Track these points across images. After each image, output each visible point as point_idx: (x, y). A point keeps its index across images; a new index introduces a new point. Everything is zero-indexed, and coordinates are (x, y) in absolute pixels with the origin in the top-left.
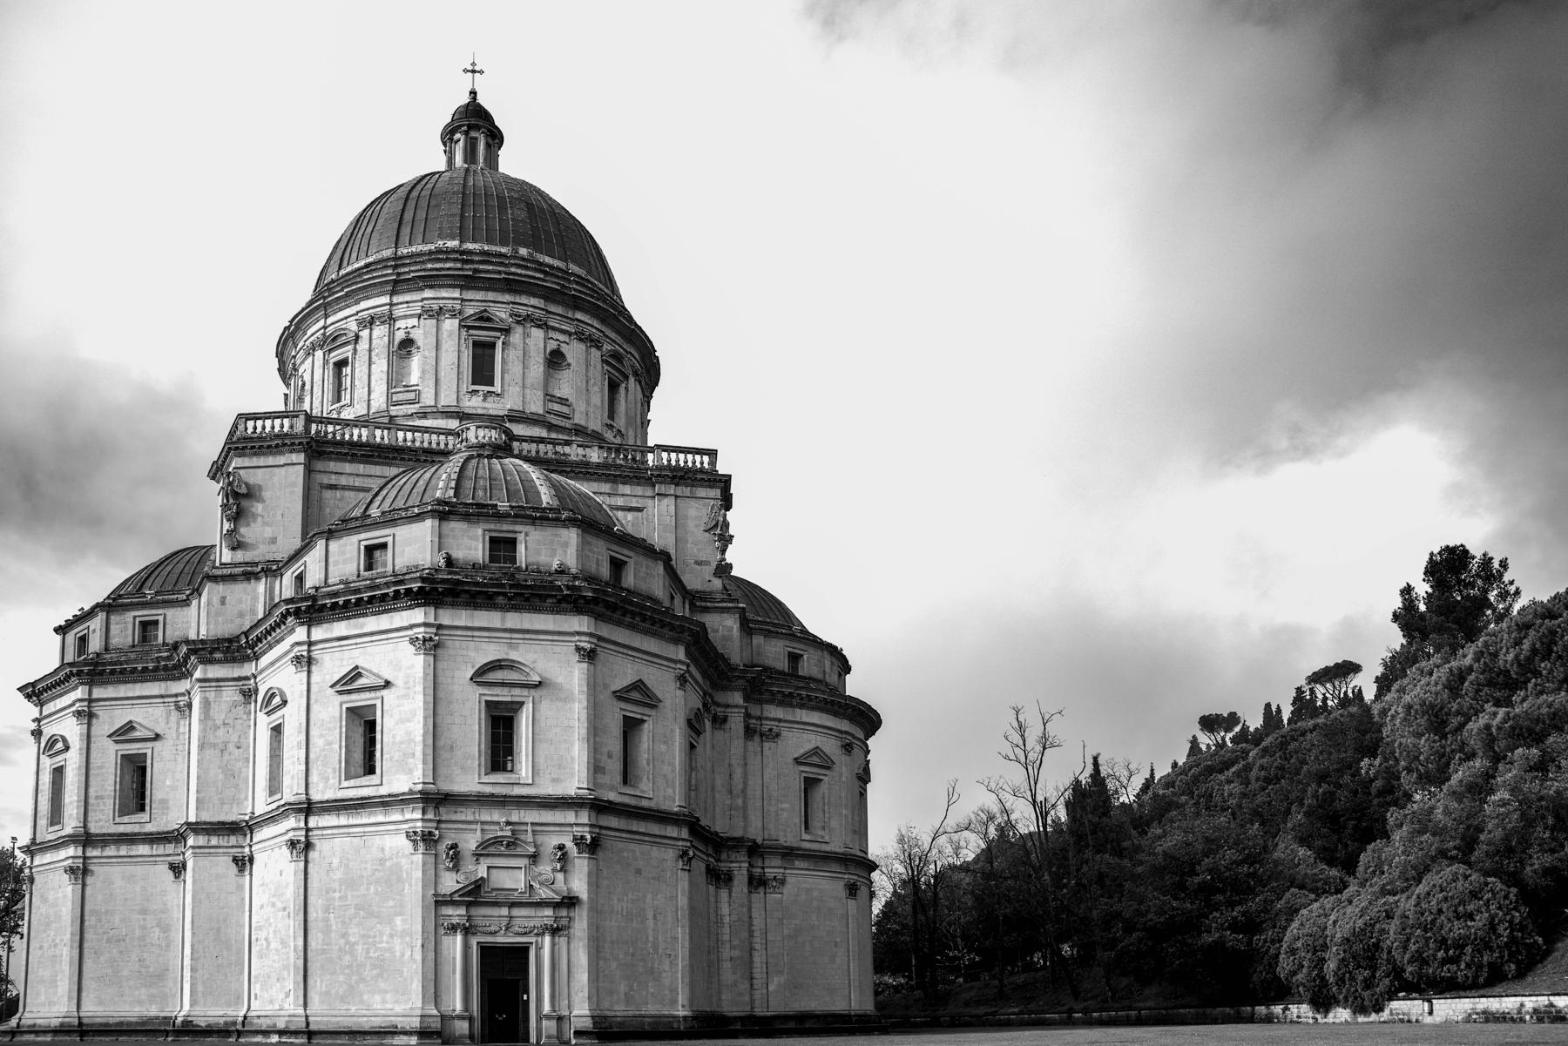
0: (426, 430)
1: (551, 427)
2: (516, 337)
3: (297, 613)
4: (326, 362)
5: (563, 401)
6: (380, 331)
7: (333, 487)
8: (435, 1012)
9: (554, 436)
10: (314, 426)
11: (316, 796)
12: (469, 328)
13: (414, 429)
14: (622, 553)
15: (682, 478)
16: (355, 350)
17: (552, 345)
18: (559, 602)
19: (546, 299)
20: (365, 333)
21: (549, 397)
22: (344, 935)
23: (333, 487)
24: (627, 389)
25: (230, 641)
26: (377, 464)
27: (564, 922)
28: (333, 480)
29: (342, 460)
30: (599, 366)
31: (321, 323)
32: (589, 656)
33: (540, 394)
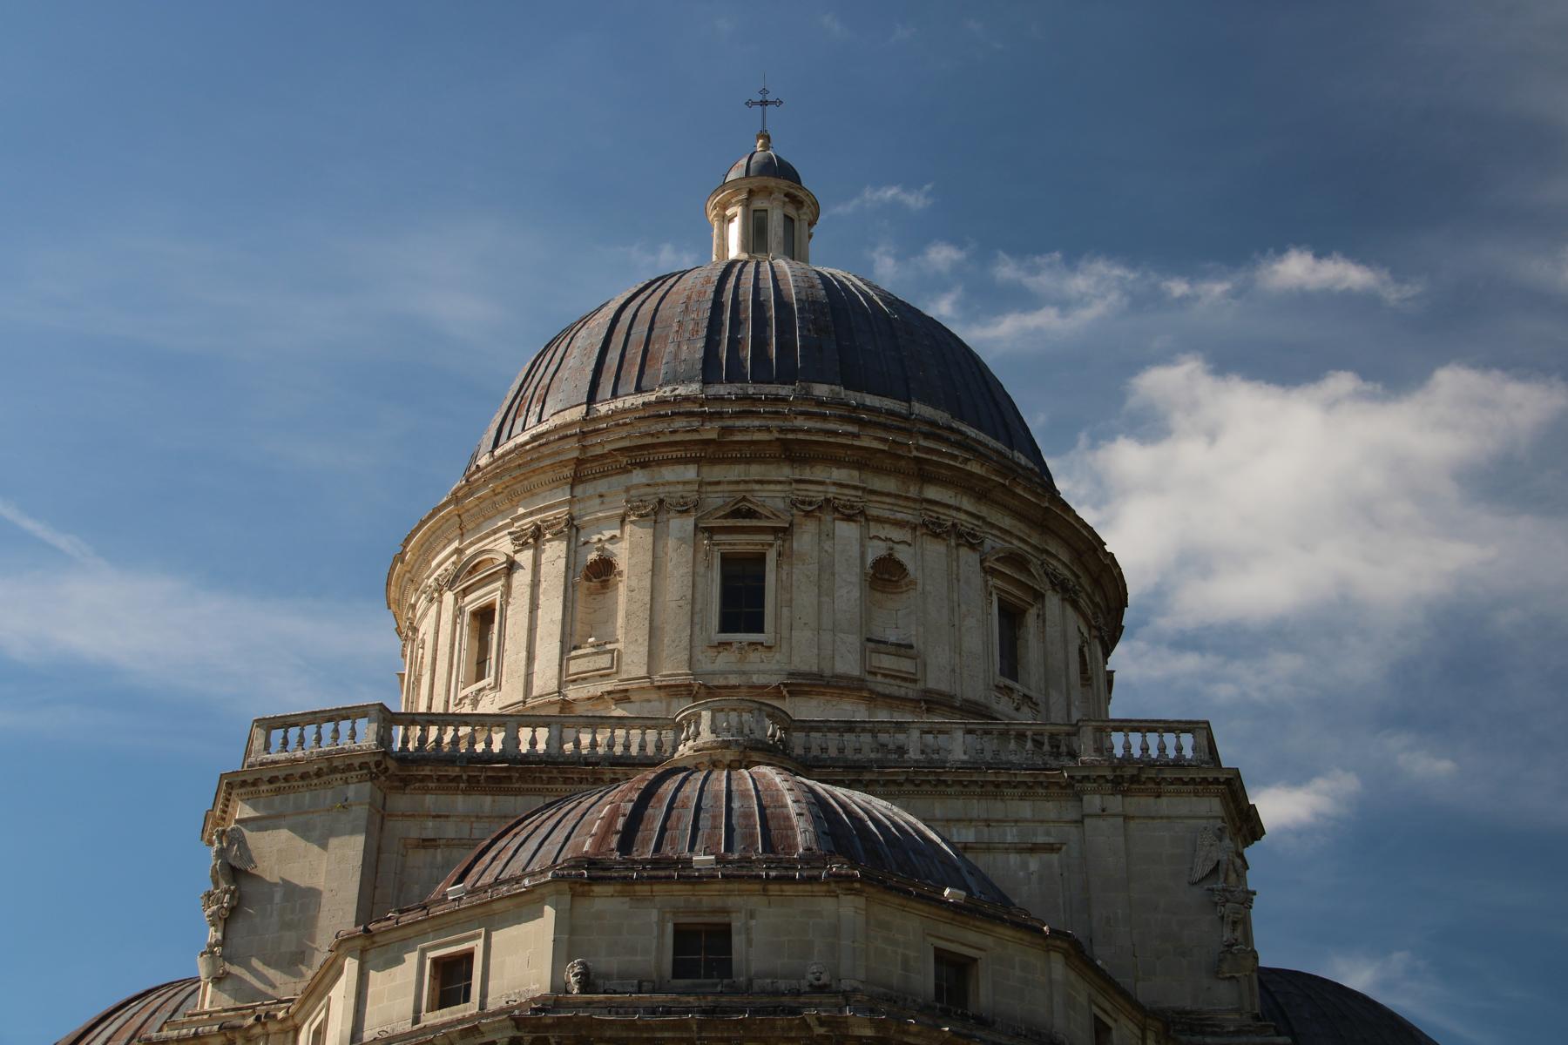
0: (620, 722)
1: (876, 698)
2: (805, 539)
4: (459, 612)
5: (903, 649)
7: (427, 843)
9: (883, 716)
10: (399, 731)
12: (711, 531)
13: (595, 723)
14: (967, 939)
15: (1134, 779)
17: (876, 550)
19: (860, 465)
20: (525, 558)
21: (874, 643)
23: (427, 843)
24: (1041, 617)
26: (518, 792)
28: (430, 829)
29: (446, 790)
30: (977, 579)
31: (456, 544)
33: (854, 640)
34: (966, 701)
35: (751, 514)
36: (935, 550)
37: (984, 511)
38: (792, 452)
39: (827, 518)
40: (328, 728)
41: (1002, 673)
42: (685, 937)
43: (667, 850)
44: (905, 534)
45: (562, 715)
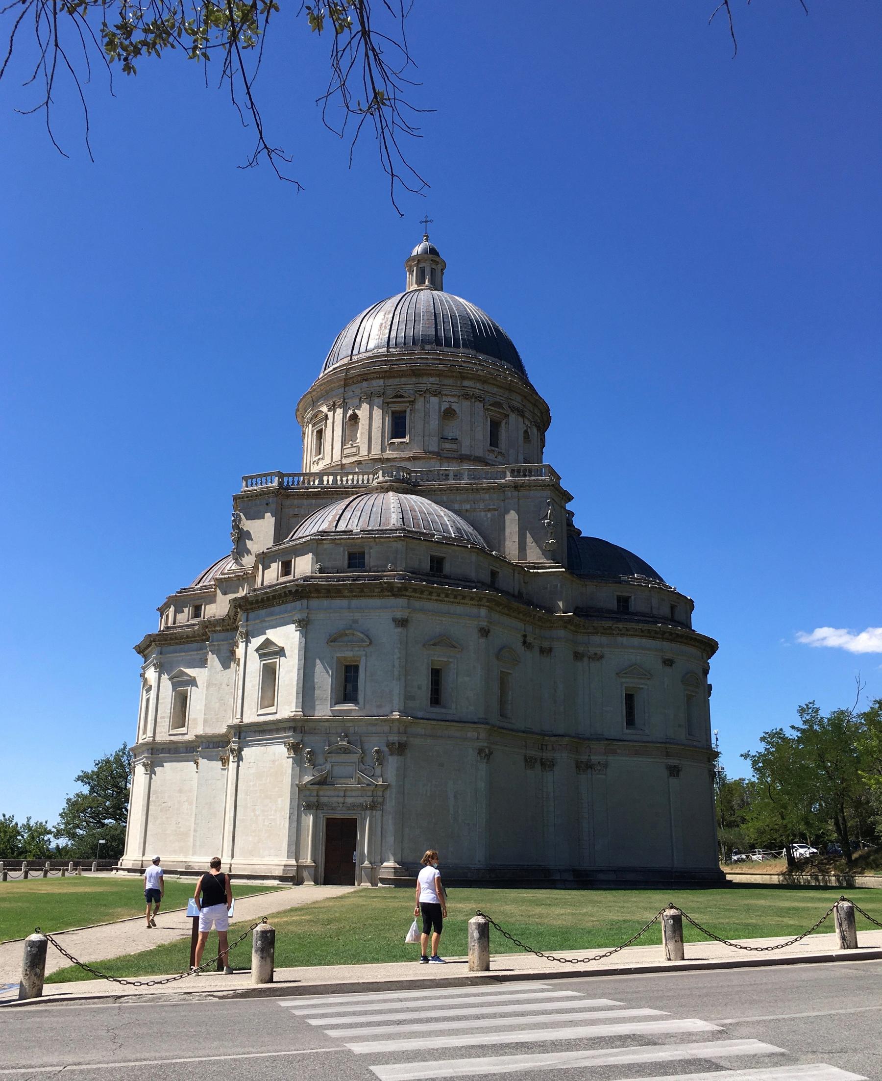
2: (419, 405)
3: (240, 606)
4: (313, 432)
6: (339, 411)
8: (294, 863)
10: (286, 479)
11: (247, 720)
12: (388, 403)
16: (326, 423)
17: (445, 406)
18: (382, 591)
19: (439, 376)
21: (444, 439)
22: (254, 810)
23: (296, 516)
25: (223, 620)
26: (323, 498)
27: (380, 800)
28: (296, 511)
32: (402, 623)
33: (436, 439)
34: (476, 457)
35: (401, 396)
36: (466, 403)
37: (486, 387)
38: (415, 373)
39: (428, 395)
40: (264, 478)
41: (491, 445)
42: (351, 556)
43: (350, 527)
44: (456, 399)
45: (342, 469)
